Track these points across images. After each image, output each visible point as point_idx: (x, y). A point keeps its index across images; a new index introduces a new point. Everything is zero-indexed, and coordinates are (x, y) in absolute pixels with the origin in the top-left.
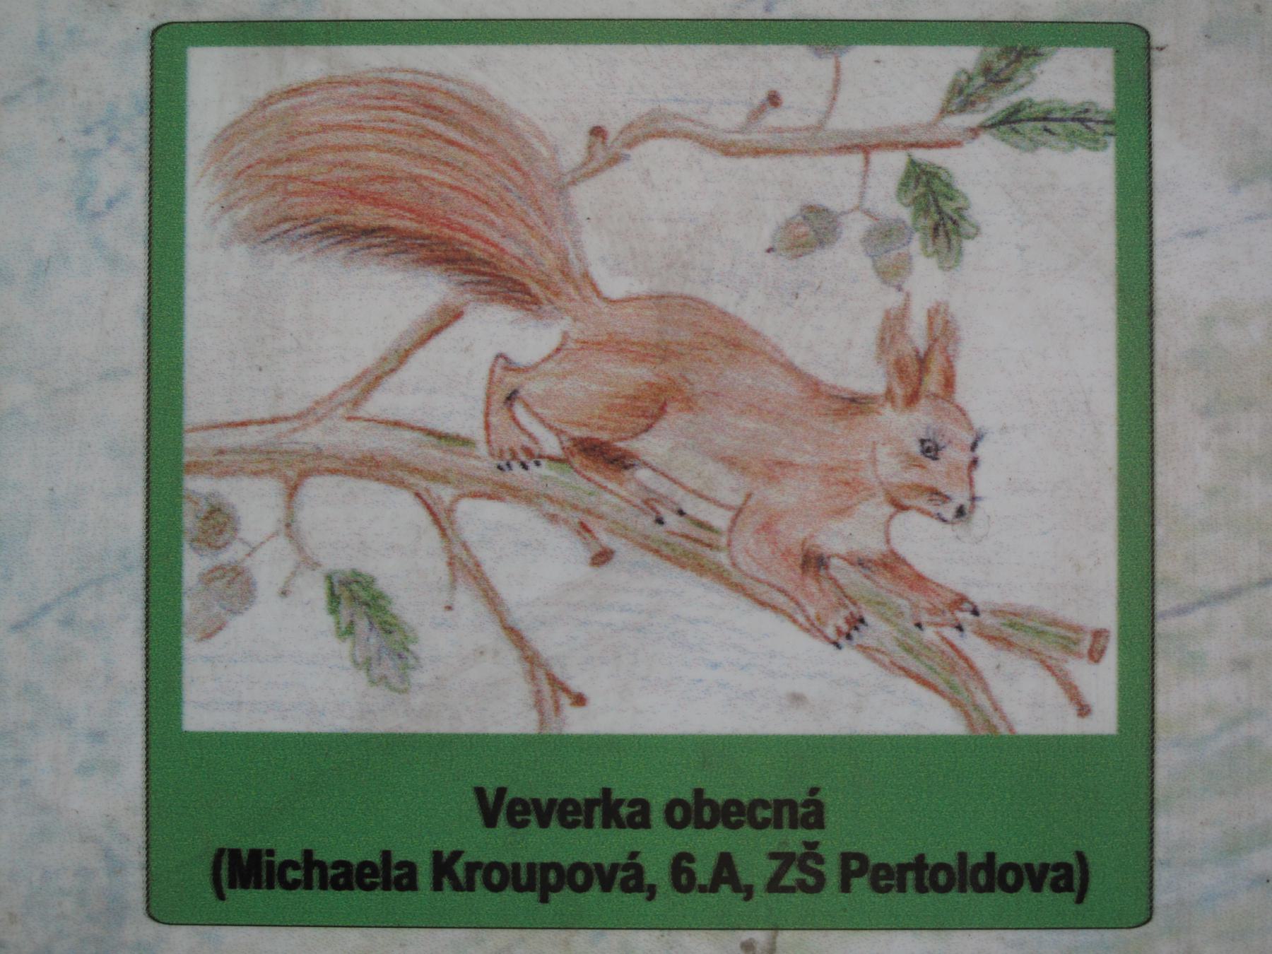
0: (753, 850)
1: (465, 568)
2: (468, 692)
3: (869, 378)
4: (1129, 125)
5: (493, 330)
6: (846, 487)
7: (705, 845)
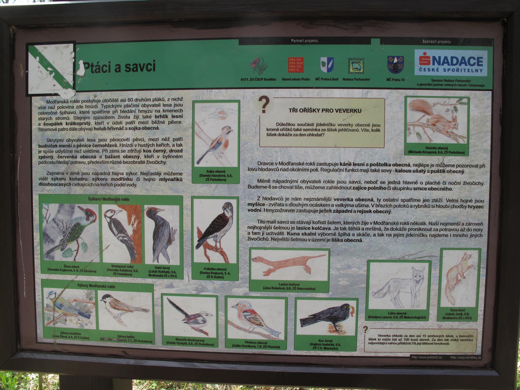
0: (443, 151)
1: (425, 132)
2: (425, 140)
3: (451, 120)
4: (468, 104)
5: (427, 117)
6: (449, 127)
7: (440, 150)
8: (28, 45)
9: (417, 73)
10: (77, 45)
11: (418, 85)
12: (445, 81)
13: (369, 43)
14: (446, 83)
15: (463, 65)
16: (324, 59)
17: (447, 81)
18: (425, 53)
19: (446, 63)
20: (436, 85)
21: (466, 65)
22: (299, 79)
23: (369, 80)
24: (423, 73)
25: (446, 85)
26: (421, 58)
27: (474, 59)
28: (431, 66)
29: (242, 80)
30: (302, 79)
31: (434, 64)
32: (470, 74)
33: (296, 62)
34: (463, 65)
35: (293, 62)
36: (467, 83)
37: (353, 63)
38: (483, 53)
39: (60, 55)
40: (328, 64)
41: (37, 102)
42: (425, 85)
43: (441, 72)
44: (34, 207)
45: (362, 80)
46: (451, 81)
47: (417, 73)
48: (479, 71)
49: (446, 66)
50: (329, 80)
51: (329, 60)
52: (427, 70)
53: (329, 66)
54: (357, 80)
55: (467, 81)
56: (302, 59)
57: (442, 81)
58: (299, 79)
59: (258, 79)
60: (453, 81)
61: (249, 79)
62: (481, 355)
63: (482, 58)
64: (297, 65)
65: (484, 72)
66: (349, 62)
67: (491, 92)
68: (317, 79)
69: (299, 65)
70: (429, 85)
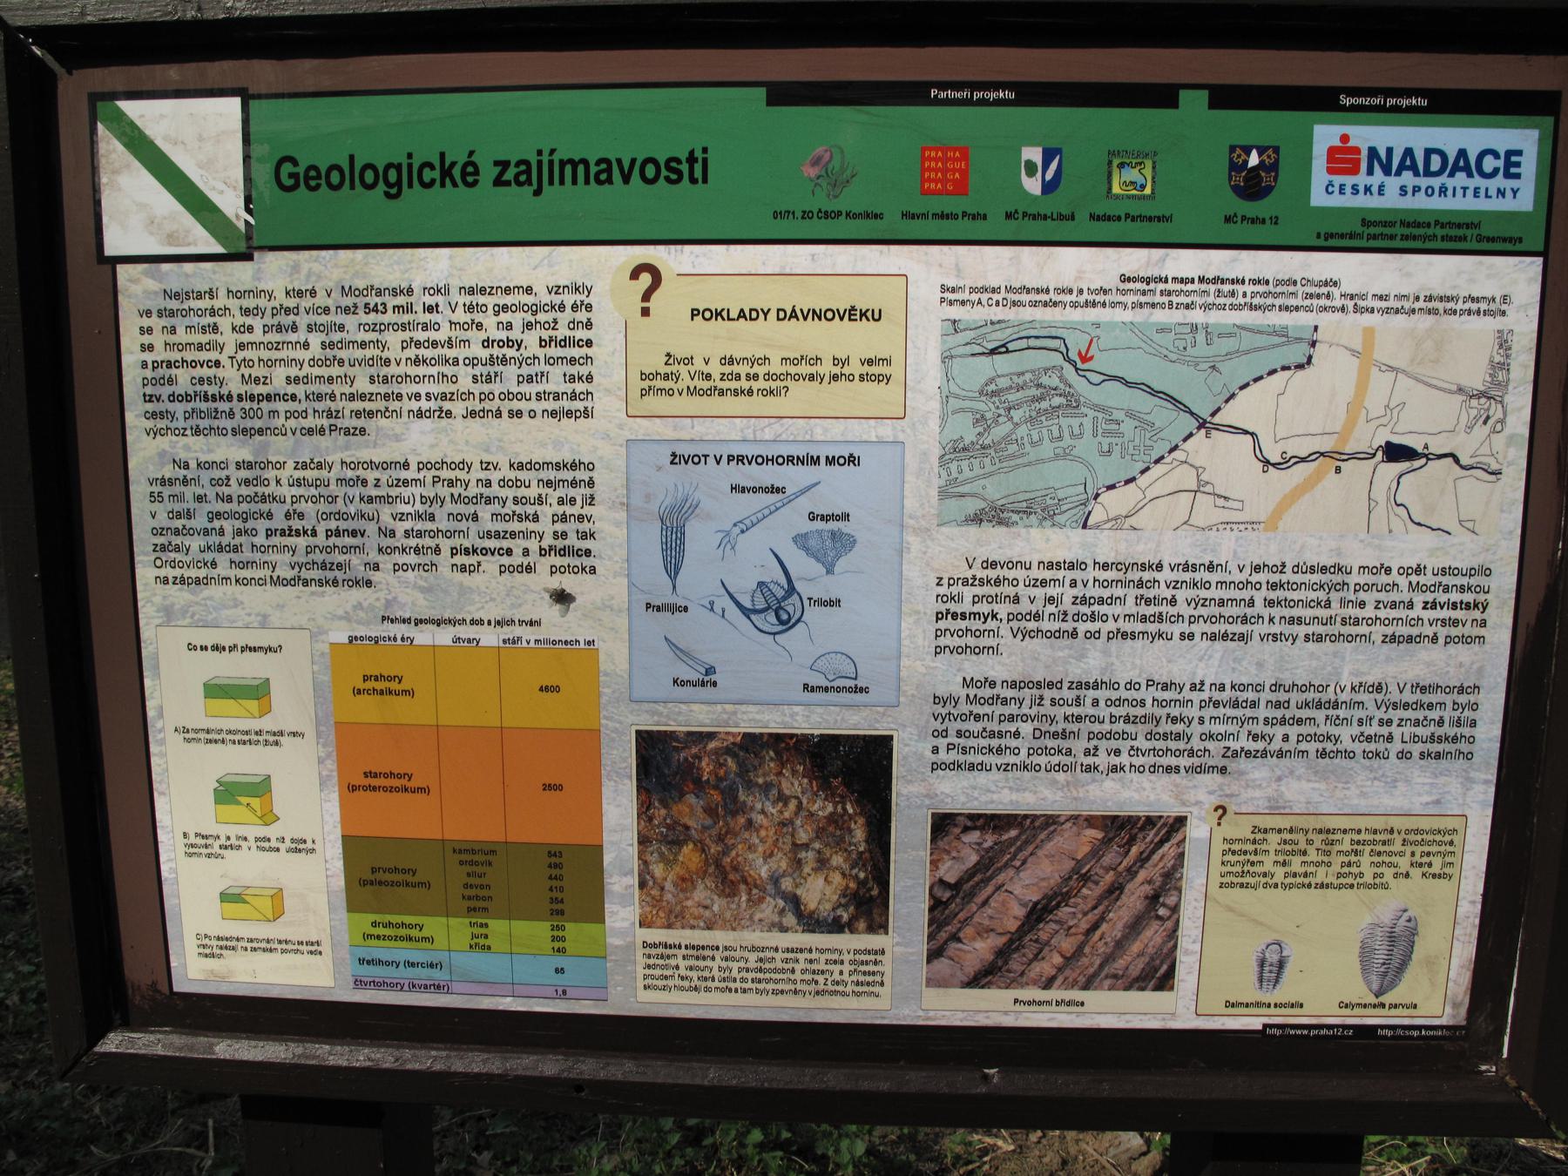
9: (1318, 198)
10: (252, 102)
11: (1319, 236)
12: (1403, 223)
13: (1172, 103)
14: (1407, 231)
15: (1461, 176)
16: (1034, 154)
18: (1345, 138)
19: (1408, 168)
20: (1375, 237)
21: (1470, 175)
22: (954, 216)
24: (1336, 201)
25: (1405, 238)
26: (1332, 151)
27: (1496, 155)
28: (1362, 179)
29: (776, 215)
30: (964, 214)
31: (1370, 172)
32: (1482, 205)
33: (945, 160)
34: (1461, 176)
35: (936, 160)
36: (1469, 233)
37: (1121, 166)
39: (202, 130)
40: (1046, 166)
41: (135, 286)
42: (1342, 236)
43: (1391, 195)
44: (140, 604)
45: (1150, 219)
46: (1419, 225)
47: (1318, 198)
48: (1509, 194)
49: (1407, 178)
50: (1045, 217)
52: (1348, 190)
53: (1049, 177)
55: (1468, 226)
56: (965, 153)
57: (1392, 224)
58: (954, 216)
59: (827, 215)
60: (1429, 225)
61: (799, 214)
63: (1519, 153)
64: (948, 171)
65: (1523, 197)
66: (1110, 163)
67: (1539, 260)
68: (1009, 216)
69: (954, 171)
70: (1352, 236)
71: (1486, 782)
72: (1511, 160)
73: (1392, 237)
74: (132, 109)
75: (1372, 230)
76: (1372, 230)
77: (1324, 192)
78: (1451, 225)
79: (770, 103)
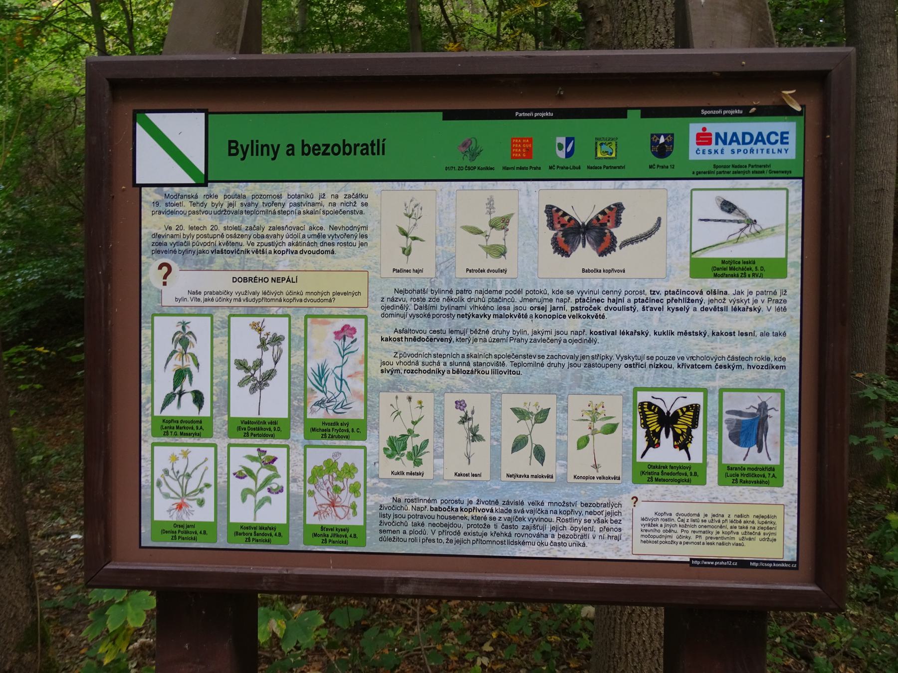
8: (136, 112)
9: (693, 156)
10: (210, 116)
12: (733, 166)
13: (625, 116)
14: (735, 170)
16: (563, 140)
17: (736, 167)
18: (704, 129)
20: (720, 173)
21: (764, 143)
22: (526, 168)
23: (623, 167)
24: (701, 157)
25: (735, 172)
26: (698, 135)
27: (776, 134)
28: (713, 147)
30: (531, 167)
31: (717, 143)
32: (771, 156)
33: (522, 143)
35: (518, 143)
36: (765, 170)
37: (601, 144)
38: (789, 126)
39: (186, 129)
41: (149, 195)
43: (728, 154)
45: (615, 168)
46: (741, 167)
47: (693, 156)
48: (783, 151)
49: (735, 146)
50: (567, 168)
51: (568, 140)
52: (707, 152)
53: (568, 150)
54: (607, 168)
56: (531, 140)
57: (729, 167)
58: (526, 168)
59: (469, 168)
62: (797, 562)
63: (787, 133)
64: (524, 149)
65: (790, 152)
68: (551, 168)
70: (709, 173)
71: (794, 431)
72: (784, 138)
73: (728, 173)
74: (153, 117)
75: (719, 170)
76: (719, 170)
77: (695, 153)
78: (756, 166)
79: (444, 119)
